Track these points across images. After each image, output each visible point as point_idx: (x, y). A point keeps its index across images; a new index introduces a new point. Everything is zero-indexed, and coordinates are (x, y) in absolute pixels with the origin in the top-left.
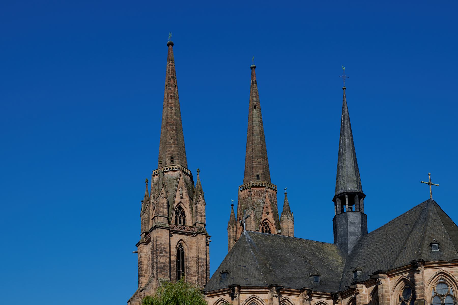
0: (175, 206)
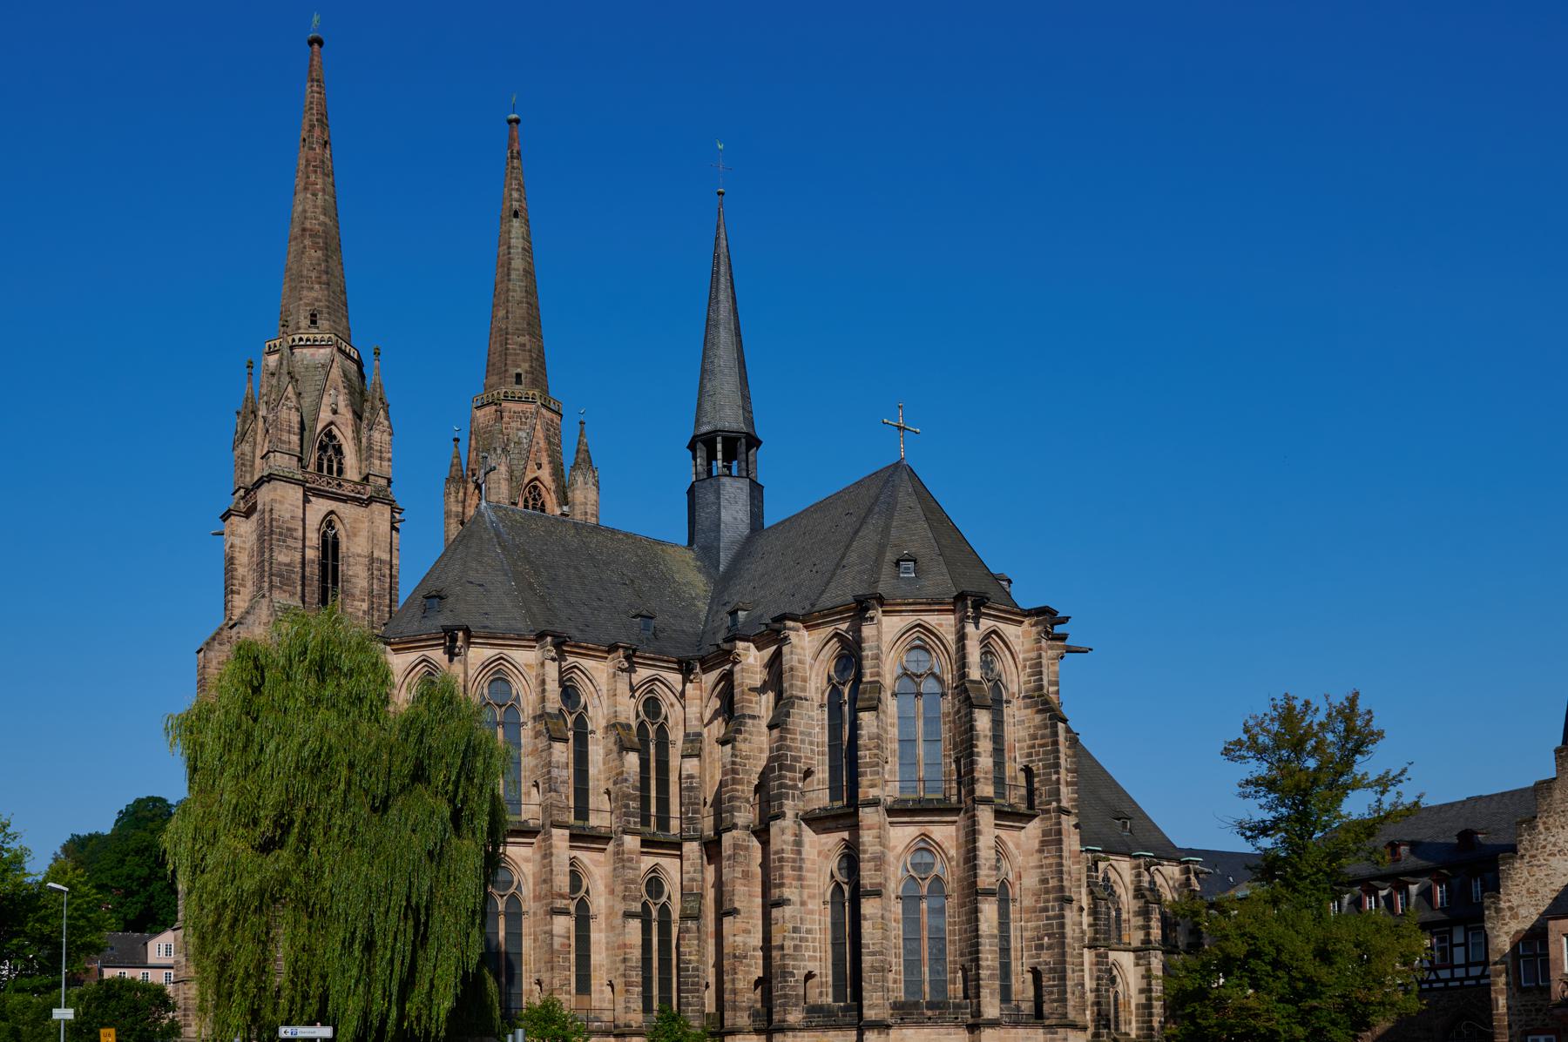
0: (318, 430)
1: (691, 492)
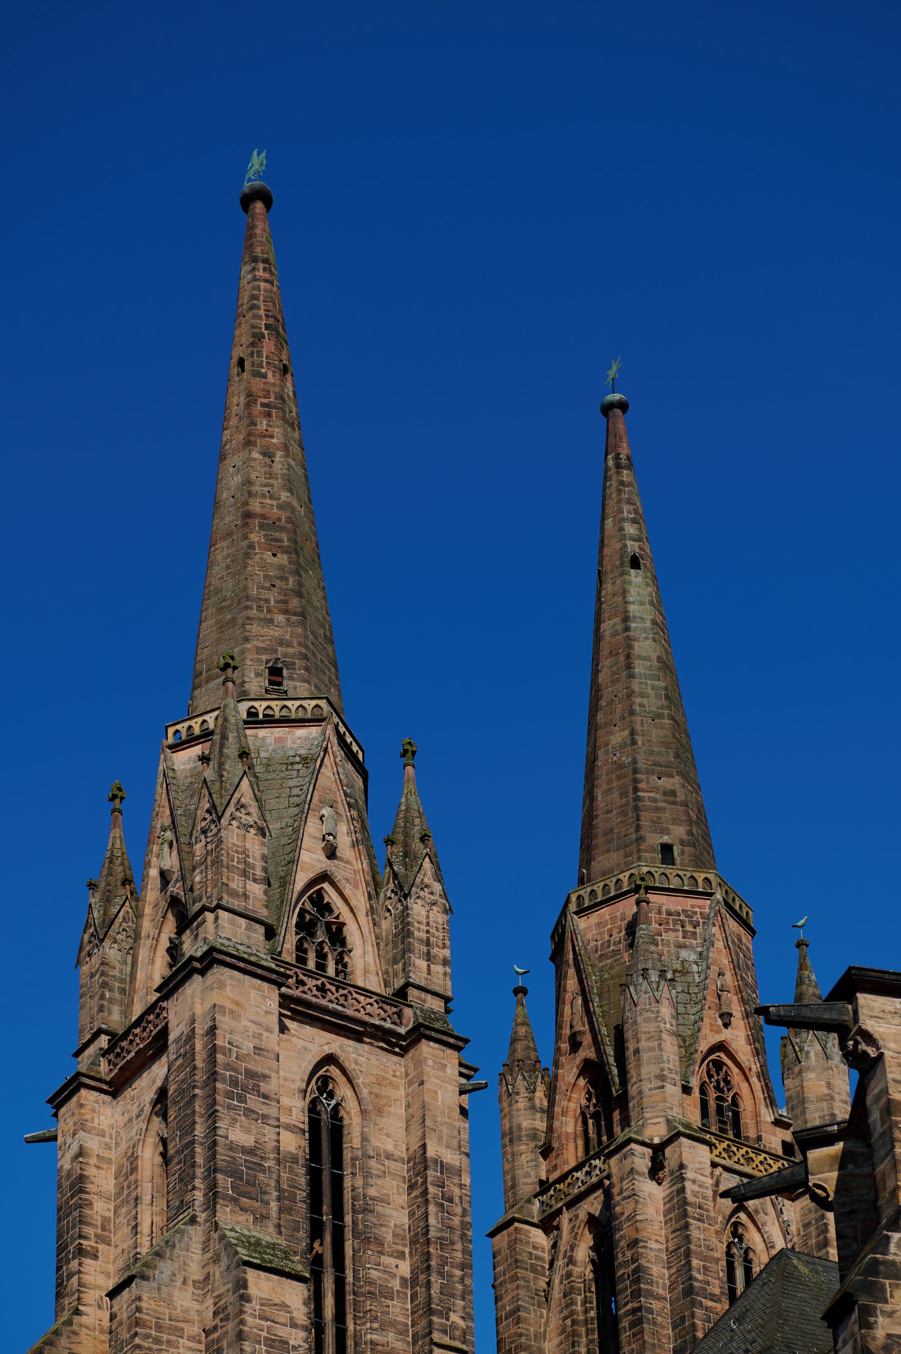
0: (299, 885)
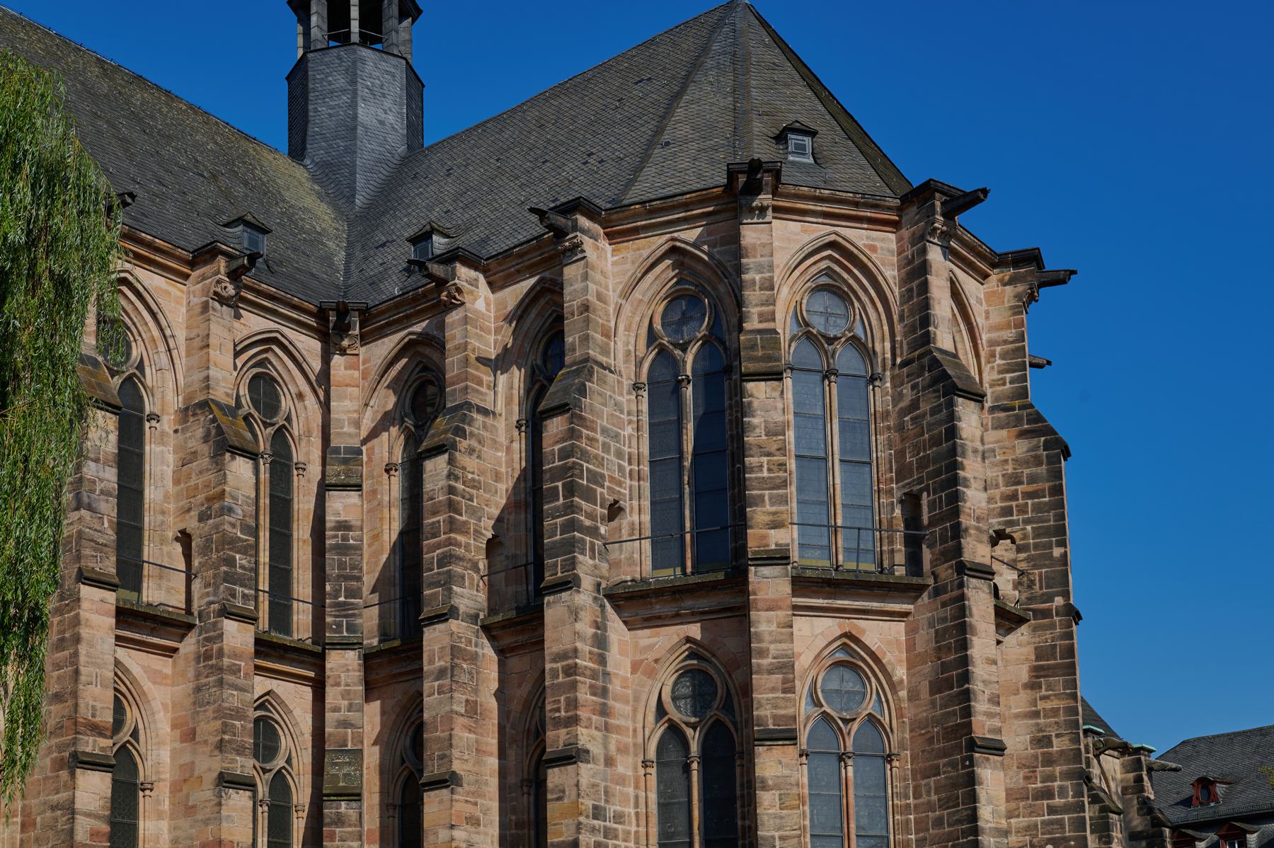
1: (298, 77)
